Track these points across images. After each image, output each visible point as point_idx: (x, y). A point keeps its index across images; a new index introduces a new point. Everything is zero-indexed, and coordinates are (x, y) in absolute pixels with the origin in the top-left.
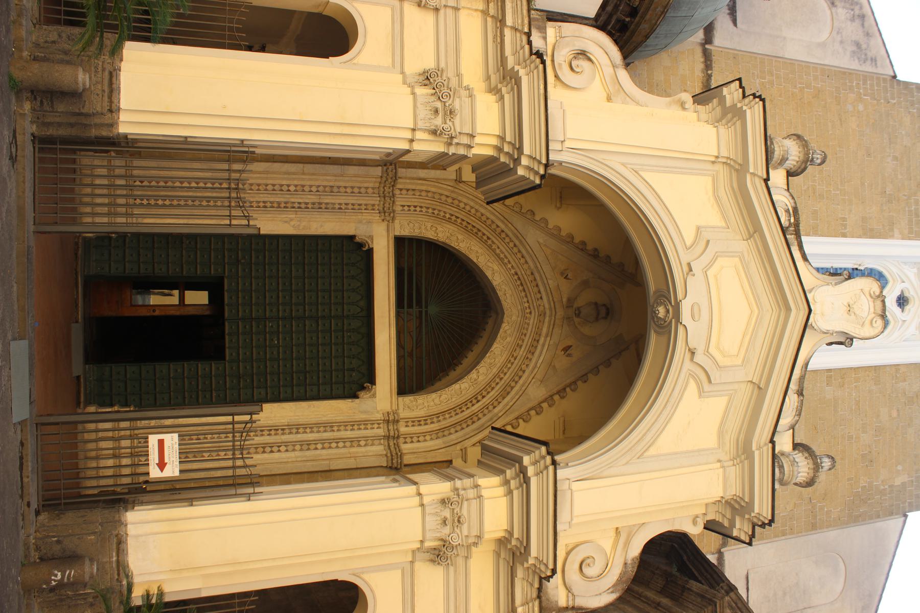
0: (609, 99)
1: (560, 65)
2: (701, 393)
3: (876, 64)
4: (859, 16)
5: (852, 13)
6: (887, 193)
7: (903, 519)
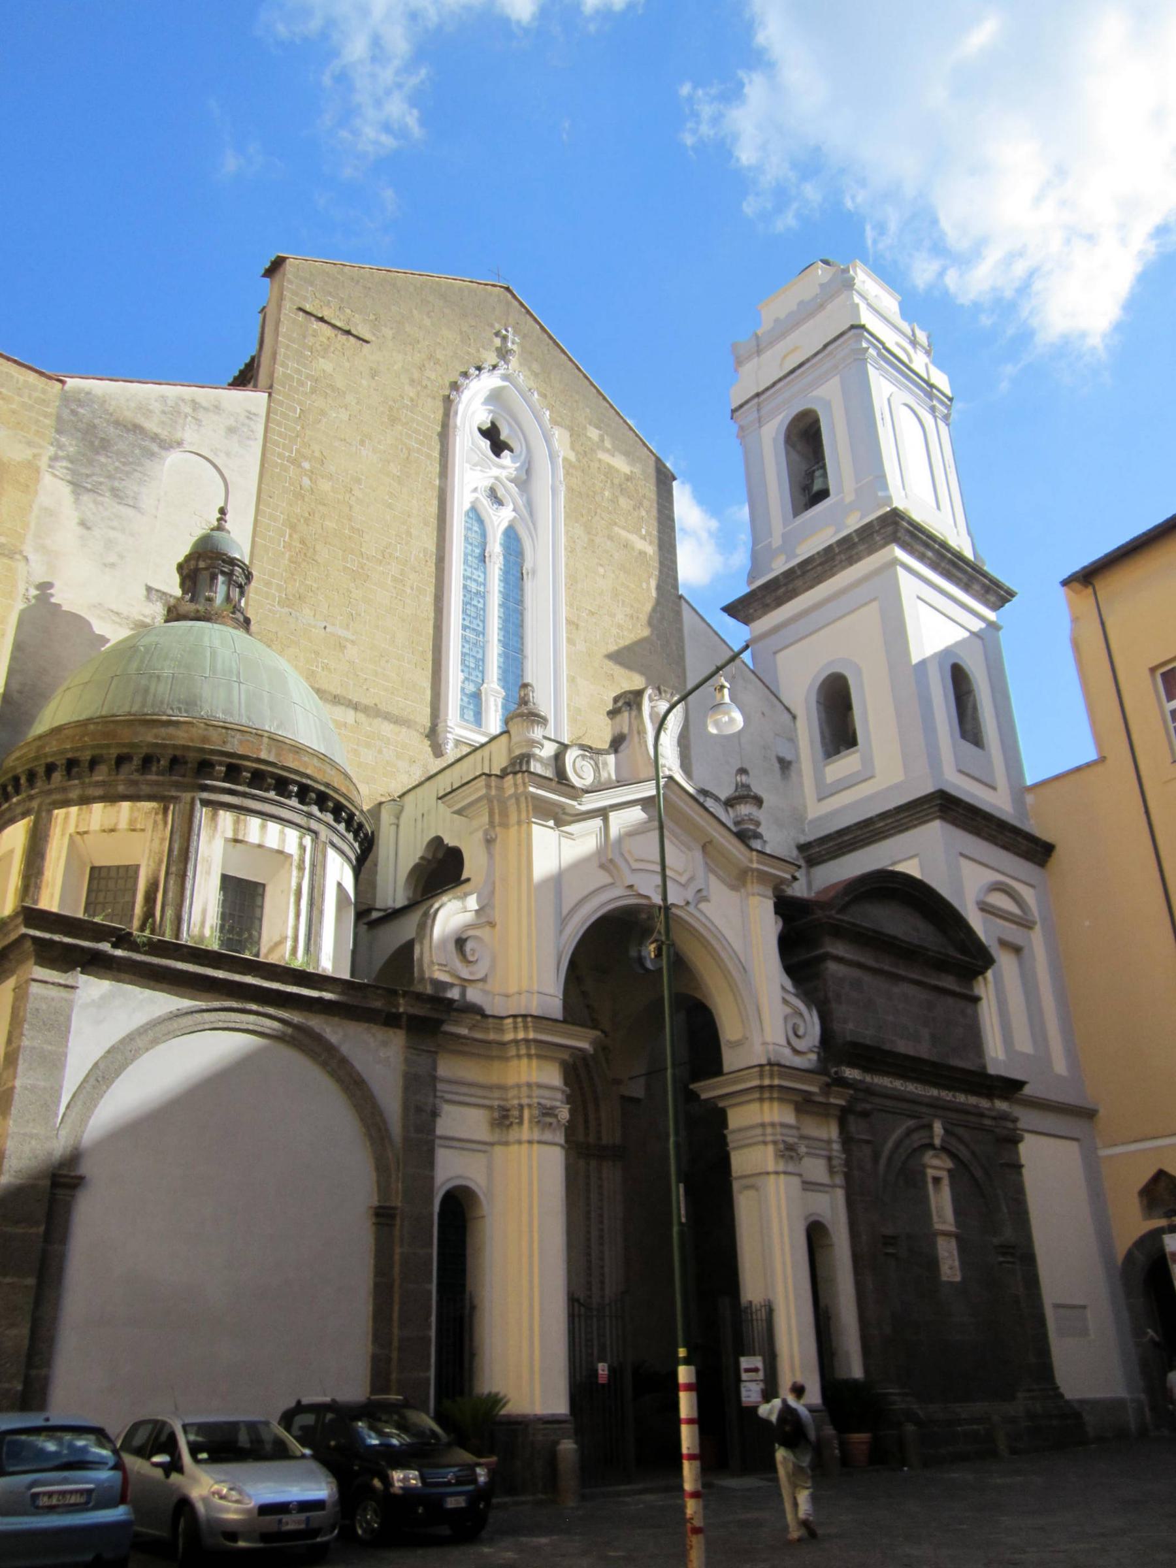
0: (492, 924)
1: (471, 973)
2: (706, 899)
3: (254, 414)
4: (194, 410)
5: (190, 418)
6: (398, 474)
7: (683, 601)
